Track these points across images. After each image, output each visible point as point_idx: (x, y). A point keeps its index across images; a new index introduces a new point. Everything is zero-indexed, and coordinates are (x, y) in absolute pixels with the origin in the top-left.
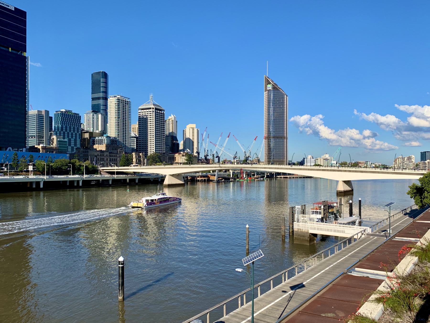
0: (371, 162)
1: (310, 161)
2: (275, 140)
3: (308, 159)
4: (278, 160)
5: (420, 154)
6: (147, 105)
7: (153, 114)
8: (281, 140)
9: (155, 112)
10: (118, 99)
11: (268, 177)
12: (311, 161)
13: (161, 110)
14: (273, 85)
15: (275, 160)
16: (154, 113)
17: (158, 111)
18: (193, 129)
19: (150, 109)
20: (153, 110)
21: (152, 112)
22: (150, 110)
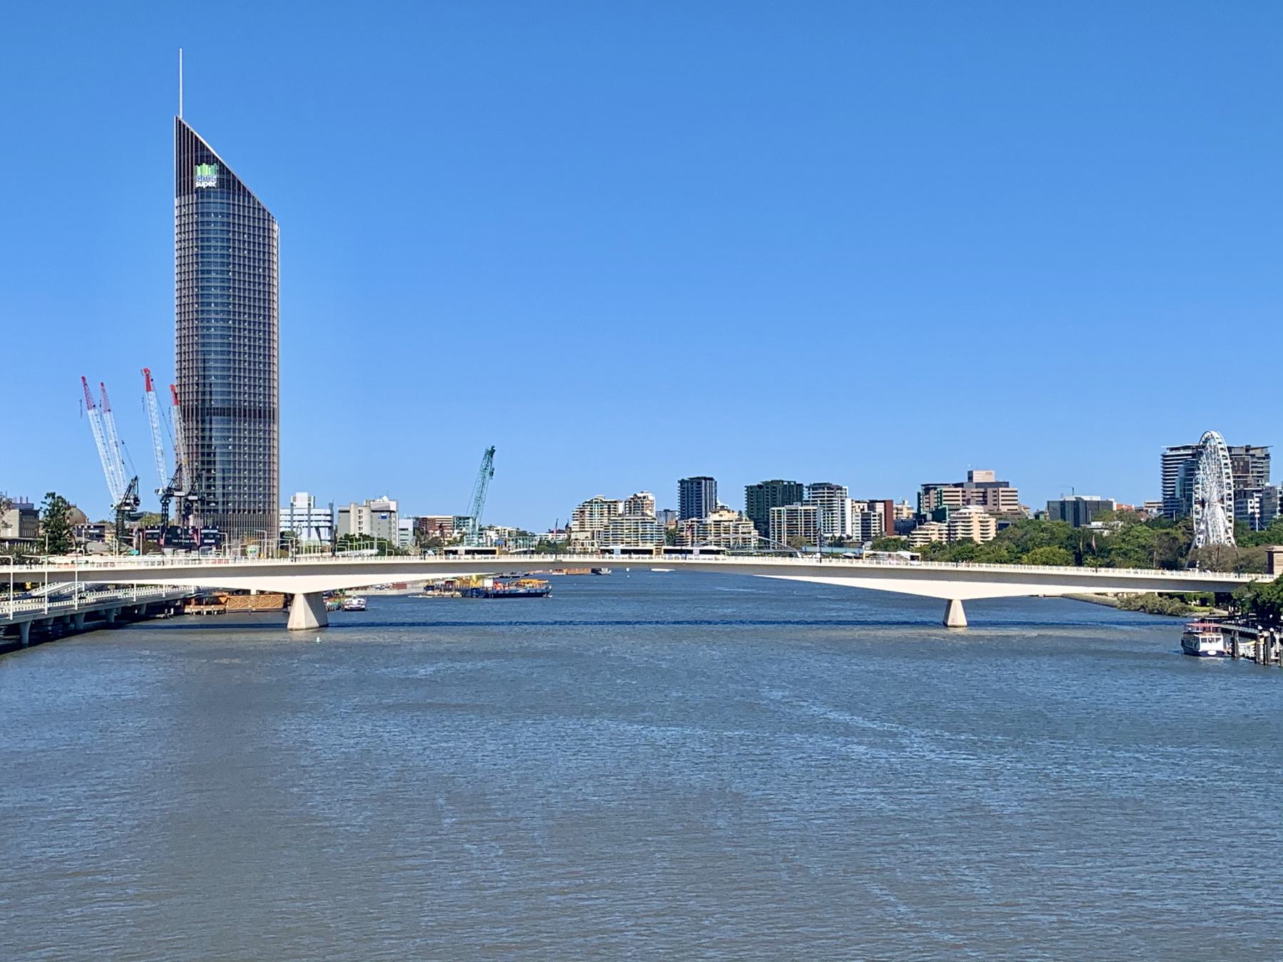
3: (295, 512)
8: (260, 423)
12: (306, 518)
14: (223, 170)
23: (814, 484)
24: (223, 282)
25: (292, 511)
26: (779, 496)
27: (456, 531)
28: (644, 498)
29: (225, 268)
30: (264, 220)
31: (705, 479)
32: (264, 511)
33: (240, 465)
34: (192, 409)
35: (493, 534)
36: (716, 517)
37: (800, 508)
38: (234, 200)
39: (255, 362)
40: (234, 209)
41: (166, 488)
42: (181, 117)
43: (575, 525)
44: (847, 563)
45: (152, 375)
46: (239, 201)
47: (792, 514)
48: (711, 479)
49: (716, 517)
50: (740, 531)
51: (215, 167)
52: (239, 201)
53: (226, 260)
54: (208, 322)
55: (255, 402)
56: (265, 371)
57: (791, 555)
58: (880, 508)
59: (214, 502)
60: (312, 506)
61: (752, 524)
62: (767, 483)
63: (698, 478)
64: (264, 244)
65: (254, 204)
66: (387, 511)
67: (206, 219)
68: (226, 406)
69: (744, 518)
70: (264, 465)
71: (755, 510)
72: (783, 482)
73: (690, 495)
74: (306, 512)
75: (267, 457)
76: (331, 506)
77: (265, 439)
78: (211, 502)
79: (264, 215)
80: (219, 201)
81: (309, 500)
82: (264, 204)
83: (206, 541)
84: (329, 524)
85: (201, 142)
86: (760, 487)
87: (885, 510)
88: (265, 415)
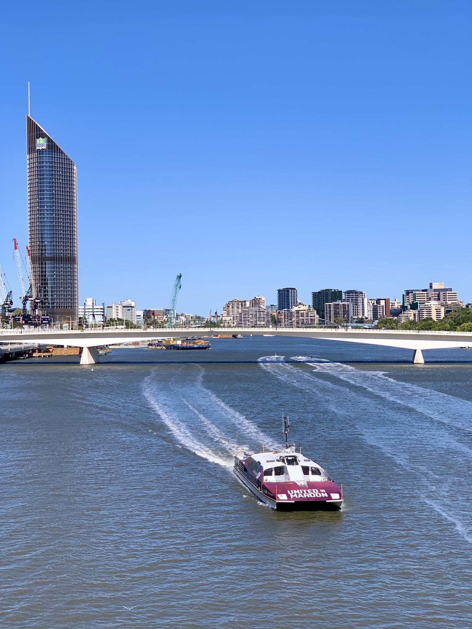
5: (276, 294)
14: (49, 140)
23: (348, 291)
24: (51, 195)
25: (85, 307)
26: (330, 297)
27: (165, 316)
28: (260, 299)
29: (51, 189)
30: (69, 164)
31: (291, 289)
32: (71, 307)
33: (59, 284)
34: (37, 258)
35: (183, 318)
36: (297, 308)
37: (340, 303)
38: (55, 155)
39: (66, 234)
40: (55, 160)
41: (24, 296)
42: (29, 115)
43: (225, 313)
44: (365, 331)
45: (17, 242)
46: (57, 155)
47: (336, 306)
48: (294, 289)
49: (297, 308)
50: (309, 315)
51: (45, 139)
52: (57, 155)
53: (51, 185)
54: (43, 215)
55: (66, 254)
56: (70, 238)
57: (335, 327)
58: (383, 303)
59: (48, 303)
60: (94, 305)
61: (315, 312)
62: (323, 291)
63: (288, 288)
64: (69, 176)
65: (64, 156)
66: (130, 307)
67: (42, 165)
68: (52, 256)
69: (311, 309)
70: (71, 285)
71: (317, 305)
72: (331, 290)
73: (283, 297)
75: (72, 281)
76: (103, 304)
77: (71, 272)
78: (46, 303)
79: (69, 162)
80: (47, 155)
81: (93, 302)
82: (69, 157)
83: (44, 322)
84: (102, 313)
85: (39, 127)
86: (319, 293)
87: (385, 304)
88: (71, 260)
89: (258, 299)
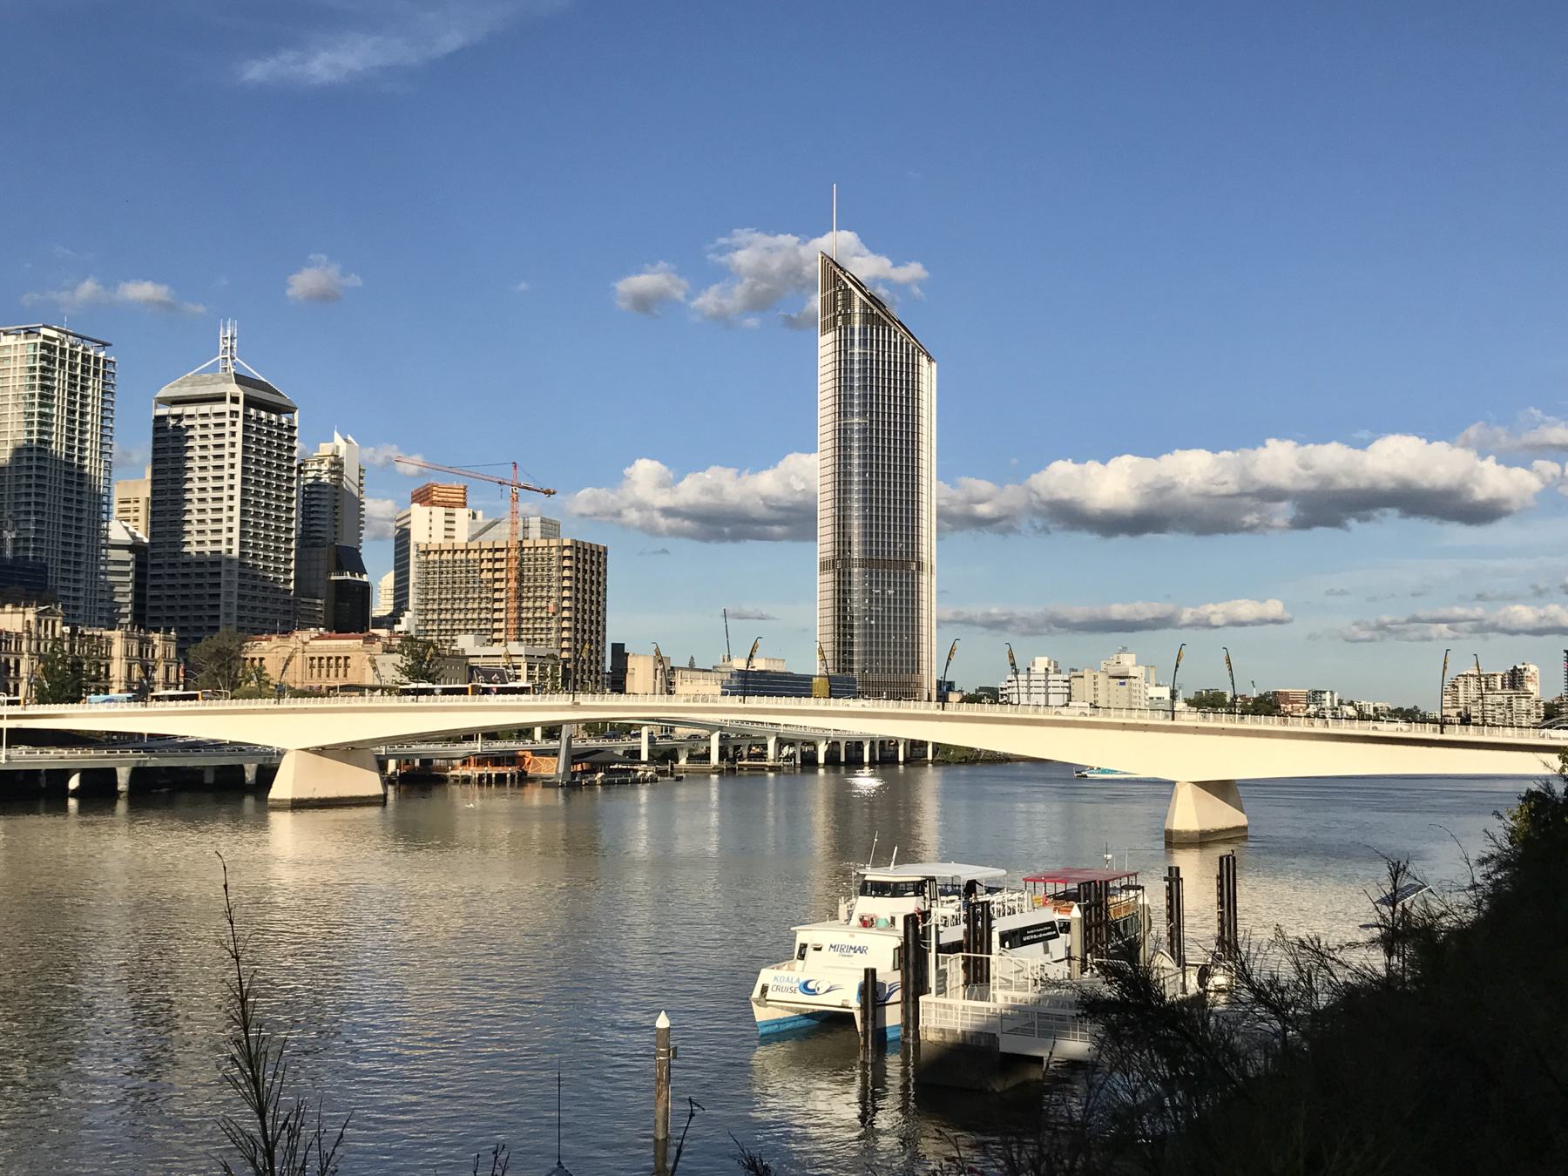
0: (1336, 695)
1: (1043, 684)
2: (871, 575)
3: (1032, 677)
4: (885, 678)
6: (203, 382)
7: (233, 429)
9: (247, 417)
10: (43, 346)
11: (832, 759)
13: (279, 409)
15: (873, 677)
16: (240, 421)
17: (263, 414)
18: (450, 511)
19: (220, 399)
20: (235, 407)
21: (227, 420)
22: (218, 408)
28: (1525, 669)
74: (1043, 677)
89: (1520, 670)
